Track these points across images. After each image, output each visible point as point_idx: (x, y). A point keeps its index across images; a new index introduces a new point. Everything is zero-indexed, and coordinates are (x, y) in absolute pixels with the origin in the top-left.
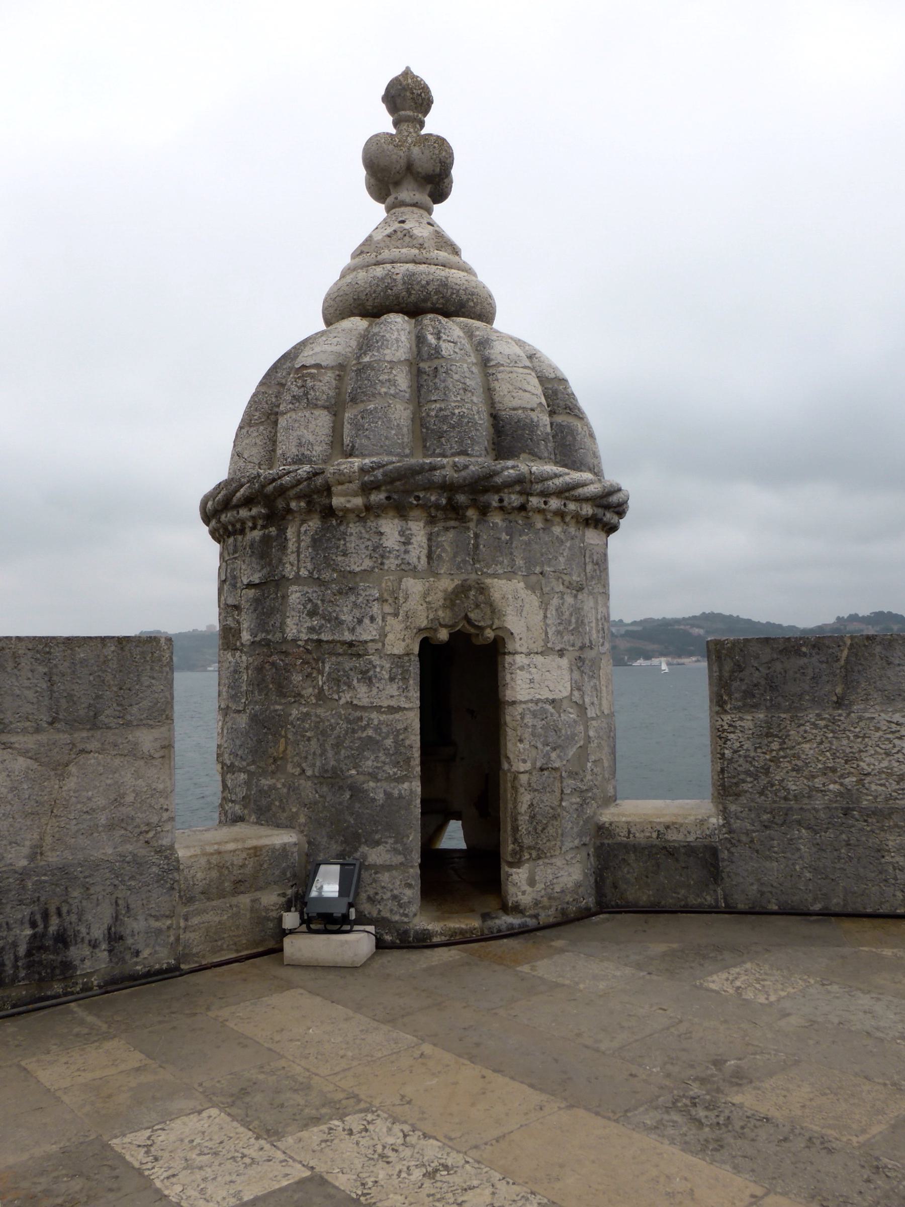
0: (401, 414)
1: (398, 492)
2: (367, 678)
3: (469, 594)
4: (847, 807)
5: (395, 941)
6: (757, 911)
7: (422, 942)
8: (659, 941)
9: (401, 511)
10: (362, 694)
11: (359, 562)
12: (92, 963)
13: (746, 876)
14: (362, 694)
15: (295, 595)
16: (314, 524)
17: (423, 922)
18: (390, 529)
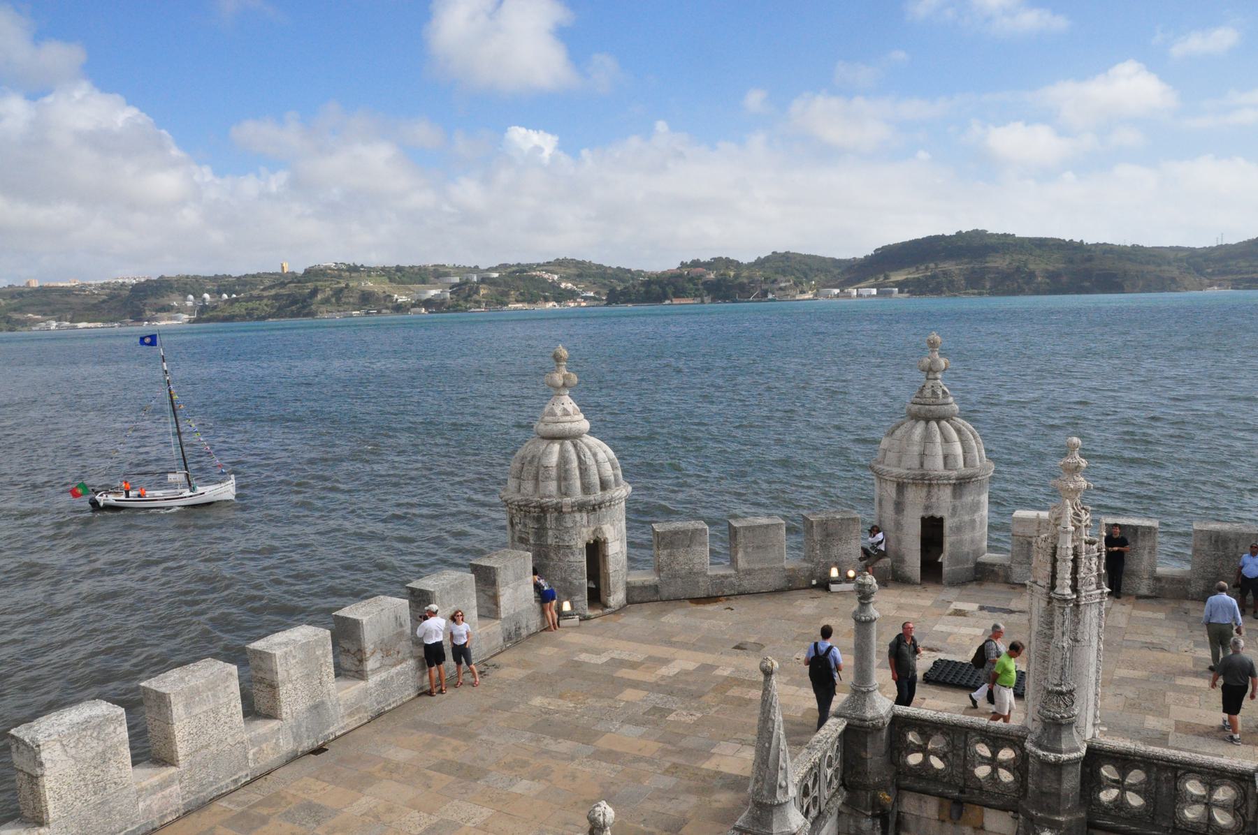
0: (578, 483)
1: (581, 507)
2: (572, 554)
3: (598, 530)
4: (691, 572)
5: (585, 618)
6: (669, 600)
7: (588, 618)
8: (648, 609)
9: (580, 511)
10: (572, 558)
11: (570, 524)
12: (524, 633)
13: (665, 593)
14: (572, 558)
15: (550, 533)
16: (556, 514)
17: (588, 613)
18: (578, 515)
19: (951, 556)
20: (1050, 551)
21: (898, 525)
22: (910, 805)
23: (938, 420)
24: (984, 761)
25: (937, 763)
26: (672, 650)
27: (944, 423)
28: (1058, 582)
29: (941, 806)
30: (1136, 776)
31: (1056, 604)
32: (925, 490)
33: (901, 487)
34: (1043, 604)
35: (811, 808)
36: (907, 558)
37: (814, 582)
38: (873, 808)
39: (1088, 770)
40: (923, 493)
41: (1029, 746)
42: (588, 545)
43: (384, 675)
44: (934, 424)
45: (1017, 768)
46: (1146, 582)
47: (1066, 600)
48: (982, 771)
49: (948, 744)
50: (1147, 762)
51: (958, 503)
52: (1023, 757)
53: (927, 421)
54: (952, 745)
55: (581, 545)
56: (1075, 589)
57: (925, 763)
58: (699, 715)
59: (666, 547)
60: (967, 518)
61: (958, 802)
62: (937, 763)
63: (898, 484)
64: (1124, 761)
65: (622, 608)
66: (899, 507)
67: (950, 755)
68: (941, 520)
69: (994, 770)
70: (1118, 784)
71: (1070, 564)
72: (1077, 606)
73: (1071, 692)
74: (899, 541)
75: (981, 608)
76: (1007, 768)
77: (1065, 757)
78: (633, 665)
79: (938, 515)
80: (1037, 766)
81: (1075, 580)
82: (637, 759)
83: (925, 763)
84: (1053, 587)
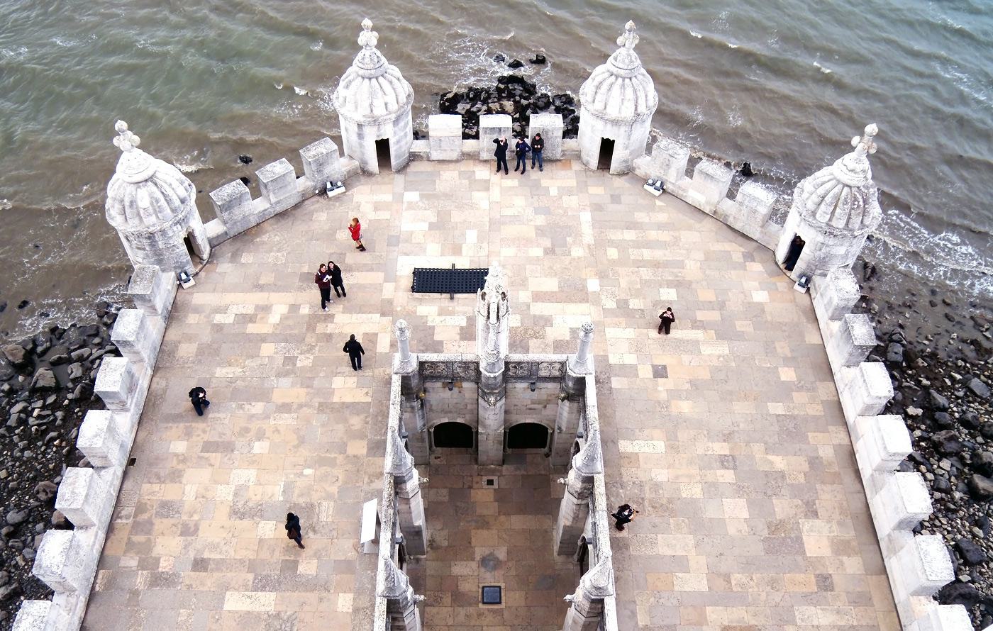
4: (244, 217)
10: (178, 250)
18: (175, 228)
19: (396, 156)
21: (361, 146)
26: (265, 295)
27: (381, 79)
40: (375, 128)
42: (185, 239)
43: (134, 400)
51: (396, 129)
53: (370, 79)
55: (182, 241)
59: (226, 210)
65: (211, 255)
66: (360, 136)
74: (363, 154)
75: (422, 196)
78: (251, 319)
82: (301, 406)
84: (489, 317)
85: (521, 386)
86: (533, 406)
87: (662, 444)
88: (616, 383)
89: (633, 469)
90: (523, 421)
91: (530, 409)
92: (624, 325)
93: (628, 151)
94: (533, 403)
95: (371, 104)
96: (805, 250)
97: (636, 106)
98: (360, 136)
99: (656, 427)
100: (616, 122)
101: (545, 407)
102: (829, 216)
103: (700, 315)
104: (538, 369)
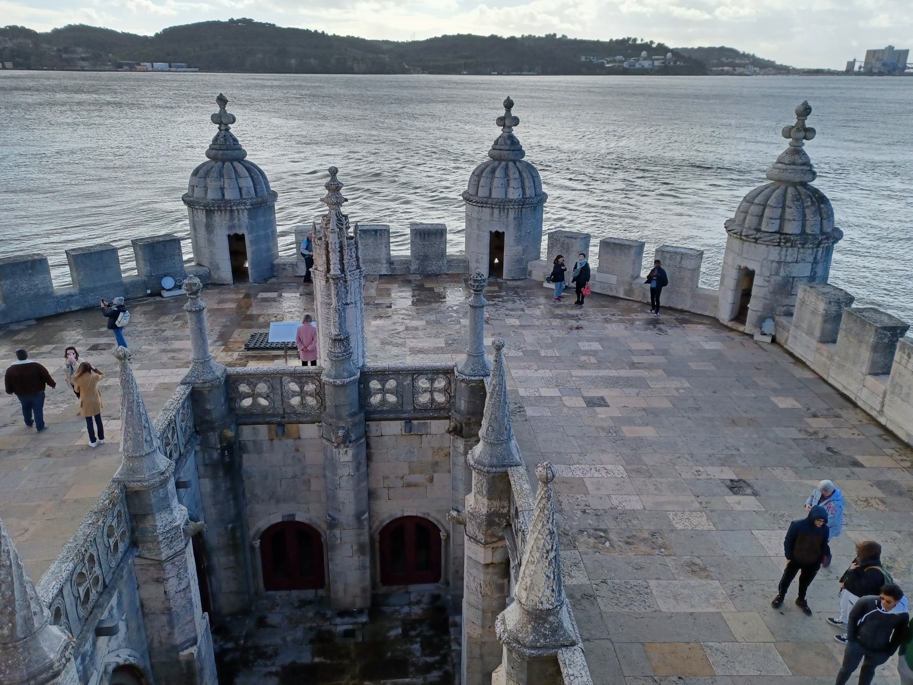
4: (36, 296)
20: (324, 246)
21: (211, 242)
22: (247, 432)
23: (232, 160)
24: (294, 394)
25: (263, 402)
27: (236, 164)
28: (332, 267)
29: (270, 430)
30: (391, 384)
31: (331, 281)
32: (228, 214)
33: (209, 212)
34: (323, 282)
35: (173, 453)
36: (220, 266)
37: (149, 292)
38: (221, 442)
39: (362, 386)
41: (324, 378)
44: (227, 164)
45: (317, 394)
46: (385, 266)
47: (338, 278)
48: (295, 401)
49: (269, 388)
50: (397, 373)
51: (254, 222)
52: (321, 385)
54: (272, 388)
56: (343, 270)
57: (255, 404)
58: (66, 406)
60: (262, 233)
61: (281, 425)
62: (263, 402)
63: (207, 210)
64: (383, 374)
66: (209, 228)
67: (271, 395)
68: (243, 235)
69: (303, 398)
70: (383, 391)
71: (338, 254)
72: (346, 282)
73: (347, 338)
76: (311, 395)
77: (348, 380)
79: (240, 233)
80: (331, 389)
81: (342, 264)
83: (255, 404)
84: (328, 270)
85: (393, 428)
86: (414, 478)
87: (621, 468)
88: (530, 412)
89: (578, 496)
90: (399, 515)
91: (409, 485)
92: (535, 367)
93: (520, 248)
94: (412, 471)
95: (222, 189)
96: (757, 281)
97: (523, 188)
98: (209, 228)
99: (604, 451)
100: (503, 205)
101: (431, 480)
102: (778, 221)
103: (636, 359)
104: (415, 391)
